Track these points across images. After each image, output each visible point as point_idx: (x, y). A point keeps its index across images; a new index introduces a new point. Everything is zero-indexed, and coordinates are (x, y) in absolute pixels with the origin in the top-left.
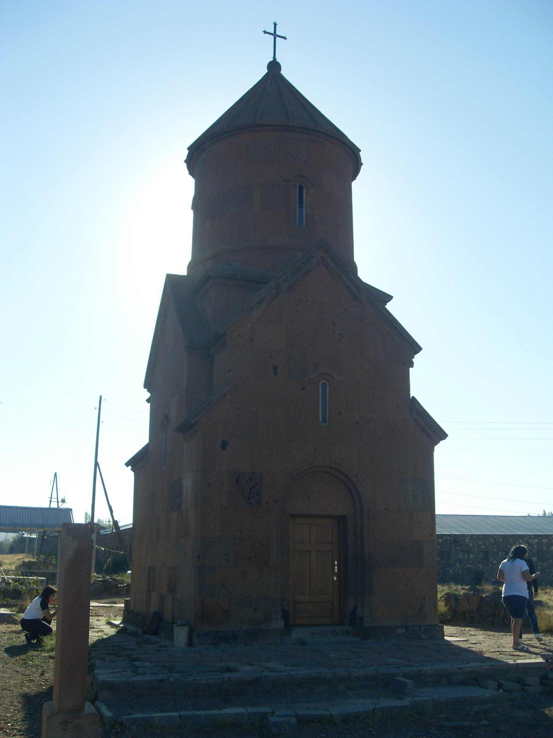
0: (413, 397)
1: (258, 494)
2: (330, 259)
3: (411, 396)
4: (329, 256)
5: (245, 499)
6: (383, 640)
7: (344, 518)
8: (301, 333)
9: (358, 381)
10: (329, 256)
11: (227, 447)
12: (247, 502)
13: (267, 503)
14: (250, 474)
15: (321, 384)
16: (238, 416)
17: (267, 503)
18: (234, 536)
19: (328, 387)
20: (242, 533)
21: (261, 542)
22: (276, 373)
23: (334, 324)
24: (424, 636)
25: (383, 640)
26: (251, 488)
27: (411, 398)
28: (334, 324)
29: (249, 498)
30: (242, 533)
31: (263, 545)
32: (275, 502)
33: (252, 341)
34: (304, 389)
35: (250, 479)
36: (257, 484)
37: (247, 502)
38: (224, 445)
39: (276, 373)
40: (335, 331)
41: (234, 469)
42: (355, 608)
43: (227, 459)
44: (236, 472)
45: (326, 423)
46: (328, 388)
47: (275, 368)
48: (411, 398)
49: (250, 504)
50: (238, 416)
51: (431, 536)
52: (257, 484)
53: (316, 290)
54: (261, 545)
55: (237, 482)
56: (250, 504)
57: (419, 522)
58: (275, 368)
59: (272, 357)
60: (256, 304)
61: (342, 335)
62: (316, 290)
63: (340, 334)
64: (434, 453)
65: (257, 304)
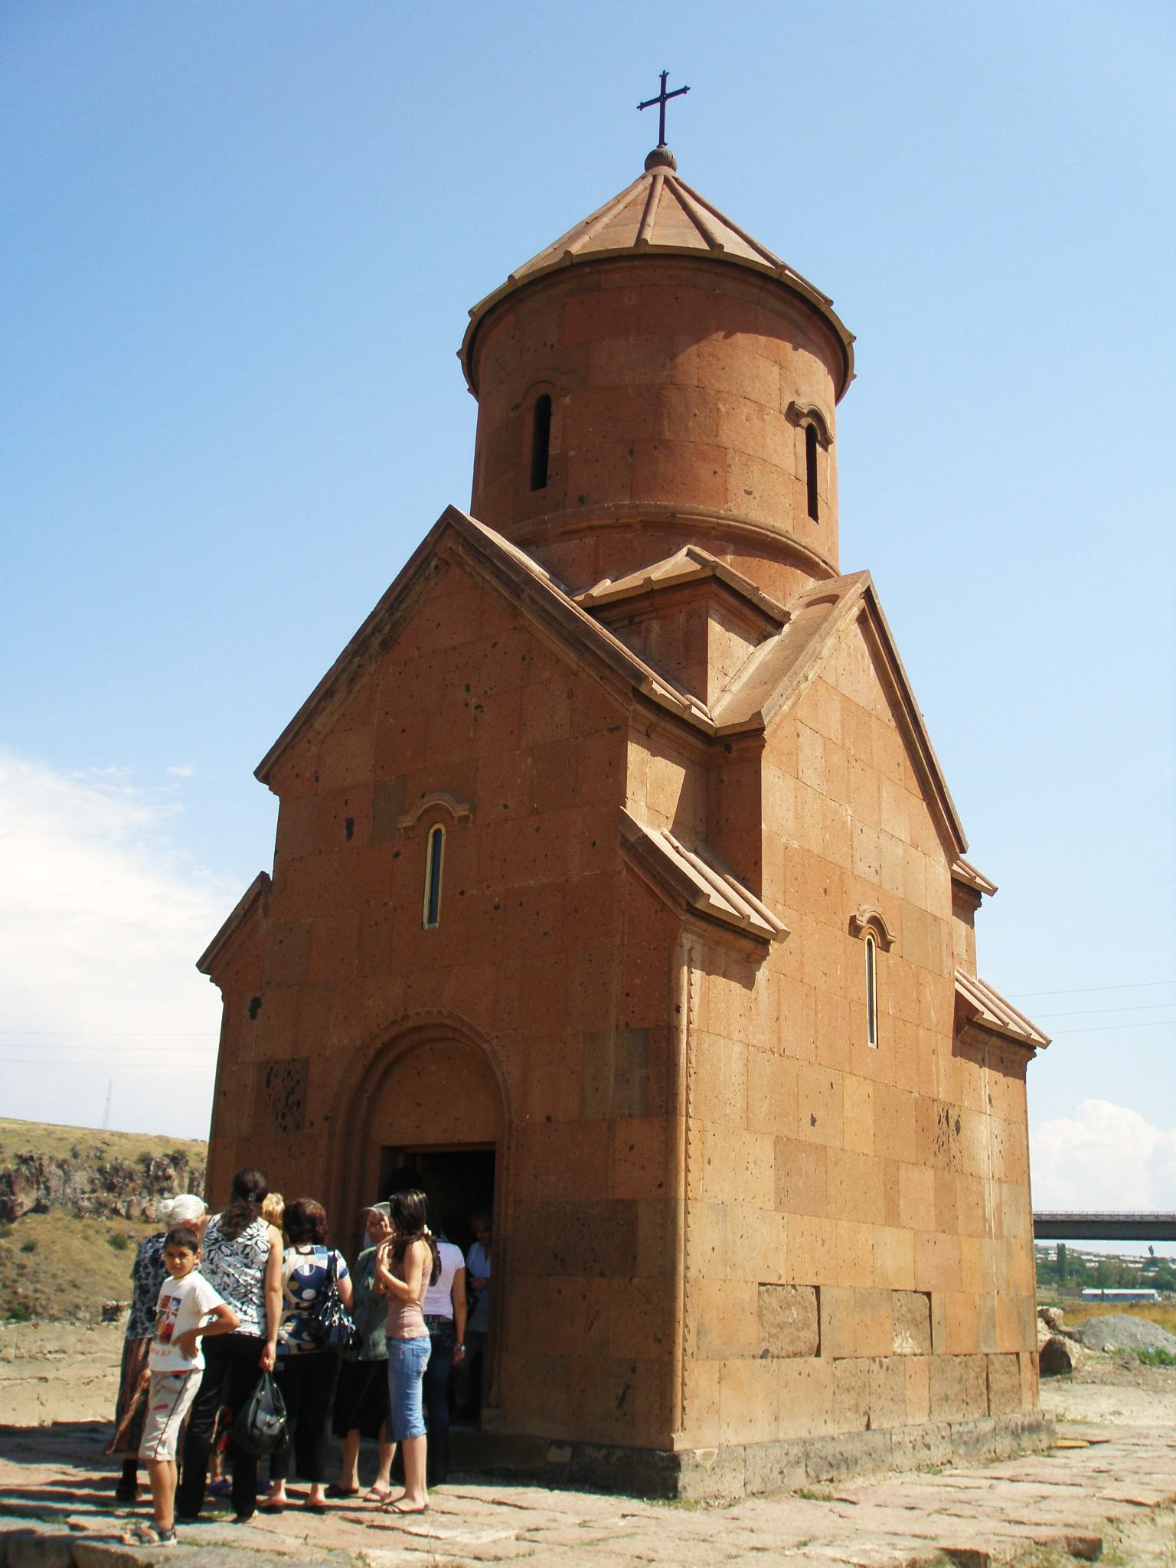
1: (298, 1104)
2: (463, 546)
5: (277, 1117)
9: (506, 806)
12: (280, 1124)
13: (312, 1124)
17: (312, 1124)
22: (350, 835)
23: (468, 689)
28: (468, 689)
29: (284, 1116)
33: (317, 779)
35: (289, 1073)
36: (298, 1082)
39: (350, 835)
51: (660, 1186)
52: (298, 1082)
55: (268, 1085)
56: (285, 1127)
57: (631, 1148)
58: (350, 823)
59: (346, 801)
61: (481, 707)
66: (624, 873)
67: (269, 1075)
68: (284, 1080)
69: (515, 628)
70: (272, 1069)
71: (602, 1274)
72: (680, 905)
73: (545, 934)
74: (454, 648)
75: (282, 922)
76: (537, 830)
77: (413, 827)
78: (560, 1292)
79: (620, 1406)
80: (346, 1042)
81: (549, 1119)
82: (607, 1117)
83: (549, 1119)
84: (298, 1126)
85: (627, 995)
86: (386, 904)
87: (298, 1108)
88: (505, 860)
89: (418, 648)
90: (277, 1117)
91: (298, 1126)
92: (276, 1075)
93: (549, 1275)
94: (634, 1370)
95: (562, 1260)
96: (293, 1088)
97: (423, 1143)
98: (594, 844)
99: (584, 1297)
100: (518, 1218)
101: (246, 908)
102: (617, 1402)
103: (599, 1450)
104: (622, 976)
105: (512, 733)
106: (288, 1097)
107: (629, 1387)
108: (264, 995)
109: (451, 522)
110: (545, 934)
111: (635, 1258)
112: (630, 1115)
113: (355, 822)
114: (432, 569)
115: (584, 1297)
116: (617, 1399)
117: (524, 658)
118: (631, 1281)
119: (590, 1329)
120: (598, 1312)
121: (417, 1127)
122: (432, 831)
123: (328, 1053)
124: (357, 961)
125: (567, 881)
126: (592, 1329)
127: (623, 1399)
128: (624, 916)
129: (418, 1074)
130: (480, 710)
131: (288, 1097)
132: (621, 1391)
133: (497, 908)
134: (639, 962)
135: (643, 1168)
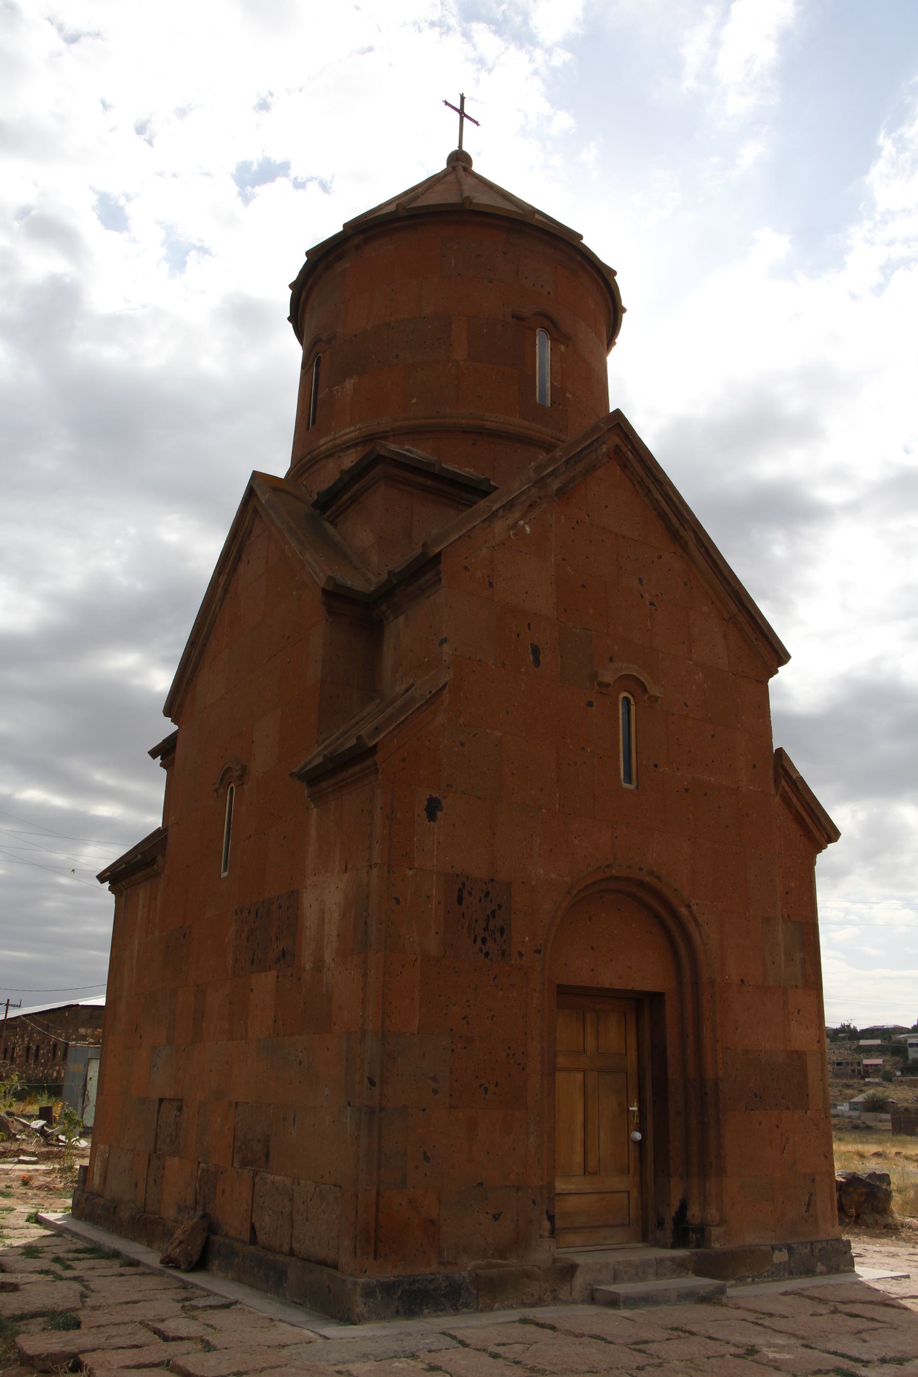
0: (780, 751)
1: (502, 931)
2: (632, 453)
3: (775, 747)
4: (629, 447)
5: (475, 940)
6: (750, 1280)
7: (656, 999)
8: (583, 586)
9: (687, 706)
10: (629, 447)
11: (439, 814)
12: (481, 950)
14: (485, 884)
15: (620, 699)
16: (462, 744)
18: (451, 1030)
19: (635, 706)
20: (468, 1023)
21: (509, 1048)
22: (537, 662)
23: (640, 581)
24: (820, 1267)
25: (750, 1280)
26: (488, 916)
27: (774, 751)
28: (640, 581)
29: (484, 941)
30: (468, 1023)
31: (514, 1055)
32: (538, 952)
33: (491, 585)
34: (590, 704)
36: (500, 907)
37: (481, 950)
38: (433, 808)
39: (537, 662)
40: (642, 596)
41: (452, 867)
42: (683, 1207)
43: (439, 843)
44: (458, 876)
45: (630, 782)
46: (633, 708)
47: (536, 651)
48: (774, 751)
49: (487, 954)
50: (462, 744)
51: (818, 1042)
52: (500, 907)
53: (606, 507)
54: (508, 1055)
55: (460, 900)
56: (487, 954)
57: (799, 1011)
58: (536, 651)
59: (529, 625)
60: (500, 508)
61: (655, 606)
62: (606, 507)
63: (651, 604)
64: (816, 867)
65: (502, 509)
66: (778, 798)
67: (460, 891)
68: (480, 900)
69: (675, 553)
70: (463, 884)
71: (787, 1108)
72: (823, 836)
73: (727, 827)
74: (624, 537)
75: (461, 721)
76: (713, 736)
77: (607, 685)
78: (761, 1124)
79: (807, 1211)
80: (553, 876)
81: (742, 981)
82: (782, 986)
83: (742, 981)
84: (503, 954)
85: (787, 893)
86: (583, 748)
87: (502, 935)
88: (689, 751)
89: (589, 516)
90: (475, 940)
91: (503, 954)
92: (470, 894)
93: (752, 1110)
94: (813, 1180)
95: (760, 1098)
96: (493, 912)
97: (599, 986)
98: (754, 766)
99: (778, 1127)
100: (726, 1063)
101: (433, 692)
102: (806, 1207)
103: (806, 1248)
104: (783, 878)
105: (684, 643)
106: (488, 921)
107: (812, 1194)
108: (444, 797)
109: (622, 424)
110: (727, 827)
111: (807, 1096)
112: (796, 987)
113: (541, 651)
114: (603, 452)
115: (778, 1127)
116: (805, 1205)
117: (686, 584)
118: (806, 1113)
119: (783, 1152)
120: (787, 1138)
121: (592, 970)
122: (620, 699)
123: (534, 883)
124: (558, 795)
125: (738, 789)
126: (785, 1151)
127: (809, 1204)
128: (780, 831)
129: (590, 919)
130: (653, 606)
131: (488, 921)
132: (808, 1198)
133: (687, 790)
134: (792, 870)
135: (807, 1028)
